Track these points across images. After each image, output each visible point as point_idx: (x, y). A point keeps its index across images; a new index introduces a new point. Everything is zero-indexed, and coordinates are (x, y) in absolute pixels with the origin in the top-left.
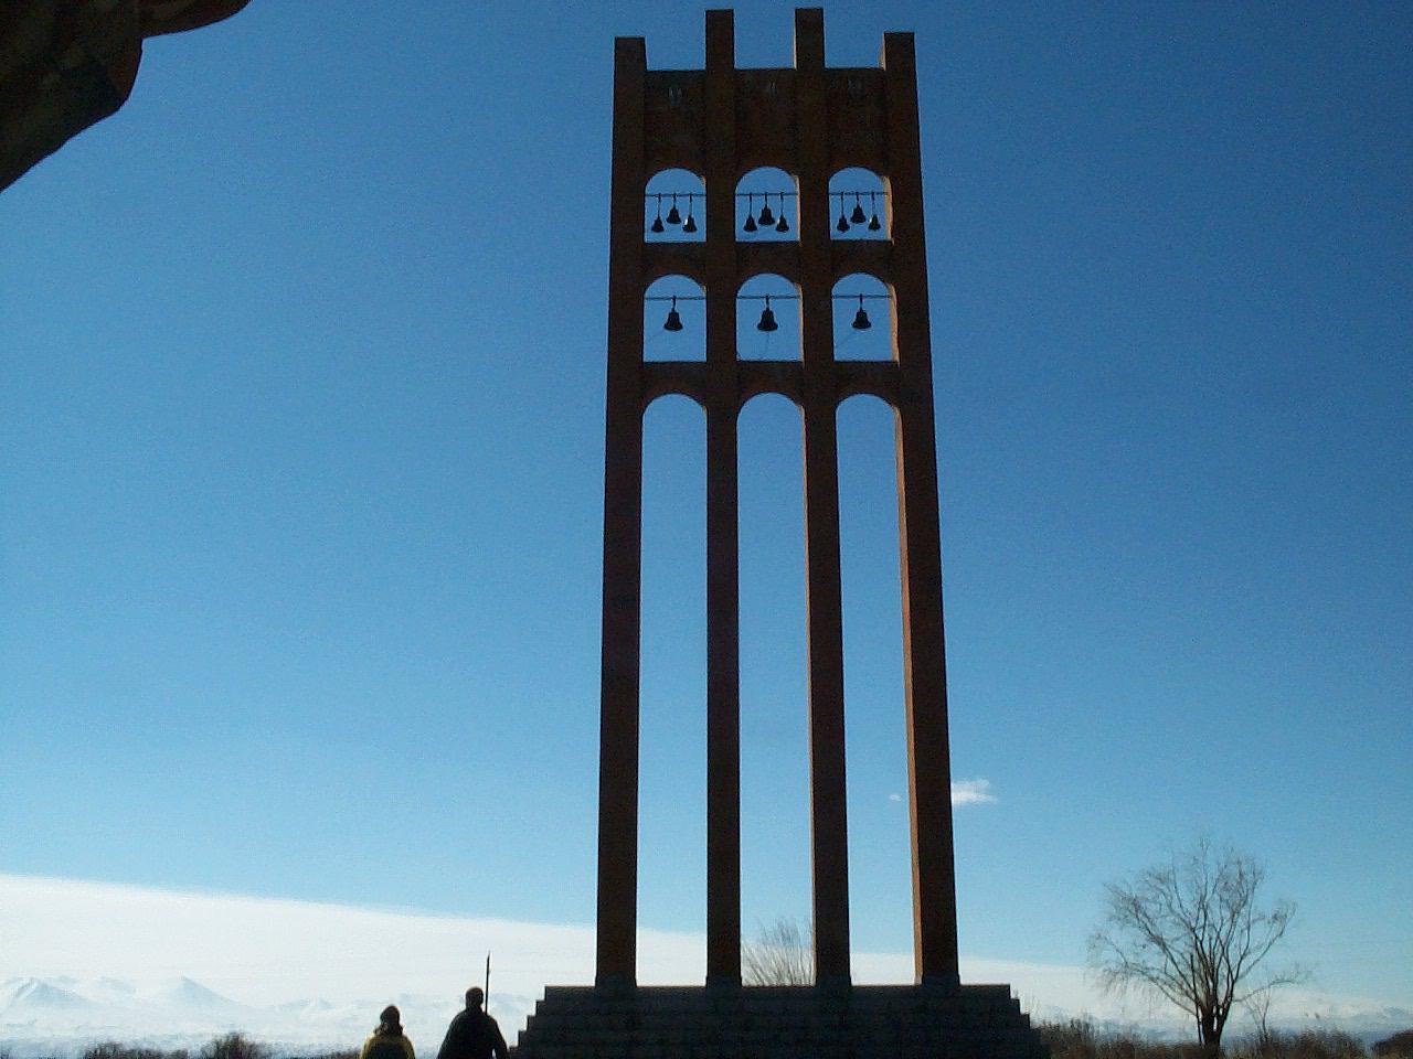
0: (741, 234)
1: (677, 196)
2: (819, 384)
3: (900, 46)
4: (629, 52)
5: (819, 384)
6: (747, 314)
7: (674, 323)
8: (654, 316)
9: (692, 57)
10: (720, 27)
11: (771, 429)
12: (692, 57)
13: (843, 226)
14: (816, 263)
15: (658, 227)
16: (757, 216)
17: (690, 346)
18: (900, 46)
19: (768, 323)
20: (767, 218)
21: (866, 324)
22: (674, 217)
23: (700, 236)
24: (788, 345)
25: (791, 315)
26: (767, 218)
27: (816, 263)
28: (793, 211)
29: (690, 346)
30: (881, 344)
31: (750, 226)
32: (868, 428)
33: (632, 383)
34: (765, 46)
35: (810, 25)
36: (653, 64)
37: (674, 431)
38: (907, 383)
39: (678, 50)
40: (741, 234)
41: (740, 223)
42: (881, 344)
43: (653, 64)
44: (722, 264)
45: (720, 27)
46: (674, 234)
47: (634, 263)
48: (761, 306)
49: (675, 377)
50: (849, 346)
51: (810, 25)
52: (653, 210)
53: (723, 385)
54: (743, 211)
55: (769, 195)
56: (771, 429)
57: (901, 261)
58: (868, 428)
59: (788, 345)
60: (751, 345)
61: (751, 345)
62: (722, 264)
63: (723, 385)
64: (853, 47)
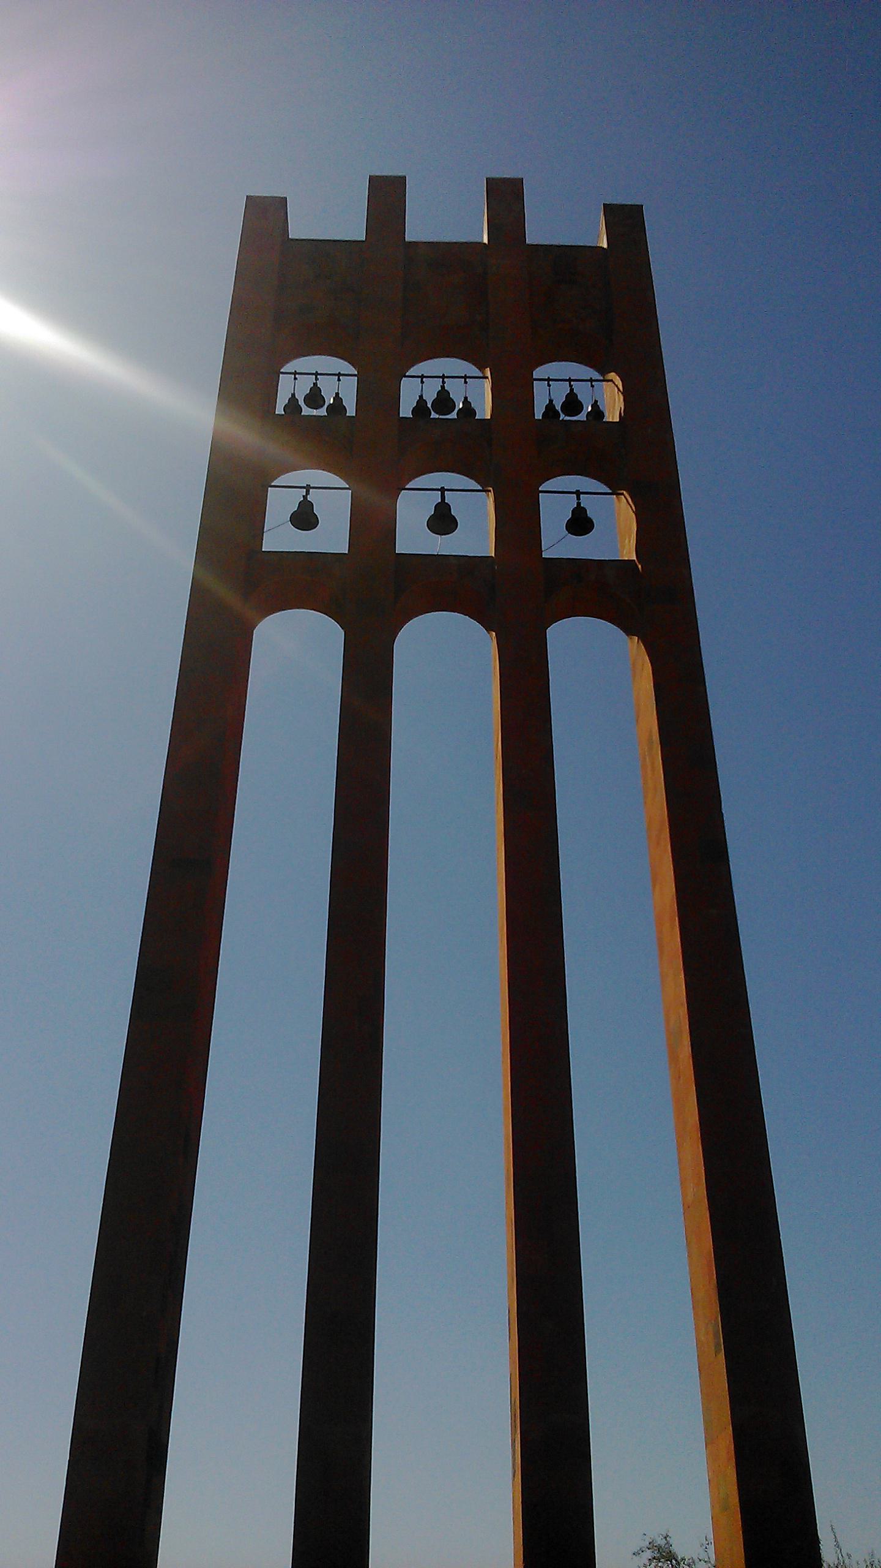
1: (325, 377)
5: (517, 598)
9: (351, 225)
11: (445, 662)
12: (351, 225)
16: (430, 398)
21: (595, 523)
30: (617, 531)
34: (447, 214)
36: (298, 230)
37: (295, 657)
39: (328, 214)
42: (617, 531)
43: (298, 230)
44: (378, 448)
48: (437, 497)
49: (301, 582)
53: (372, 595)
63: (372, 595)
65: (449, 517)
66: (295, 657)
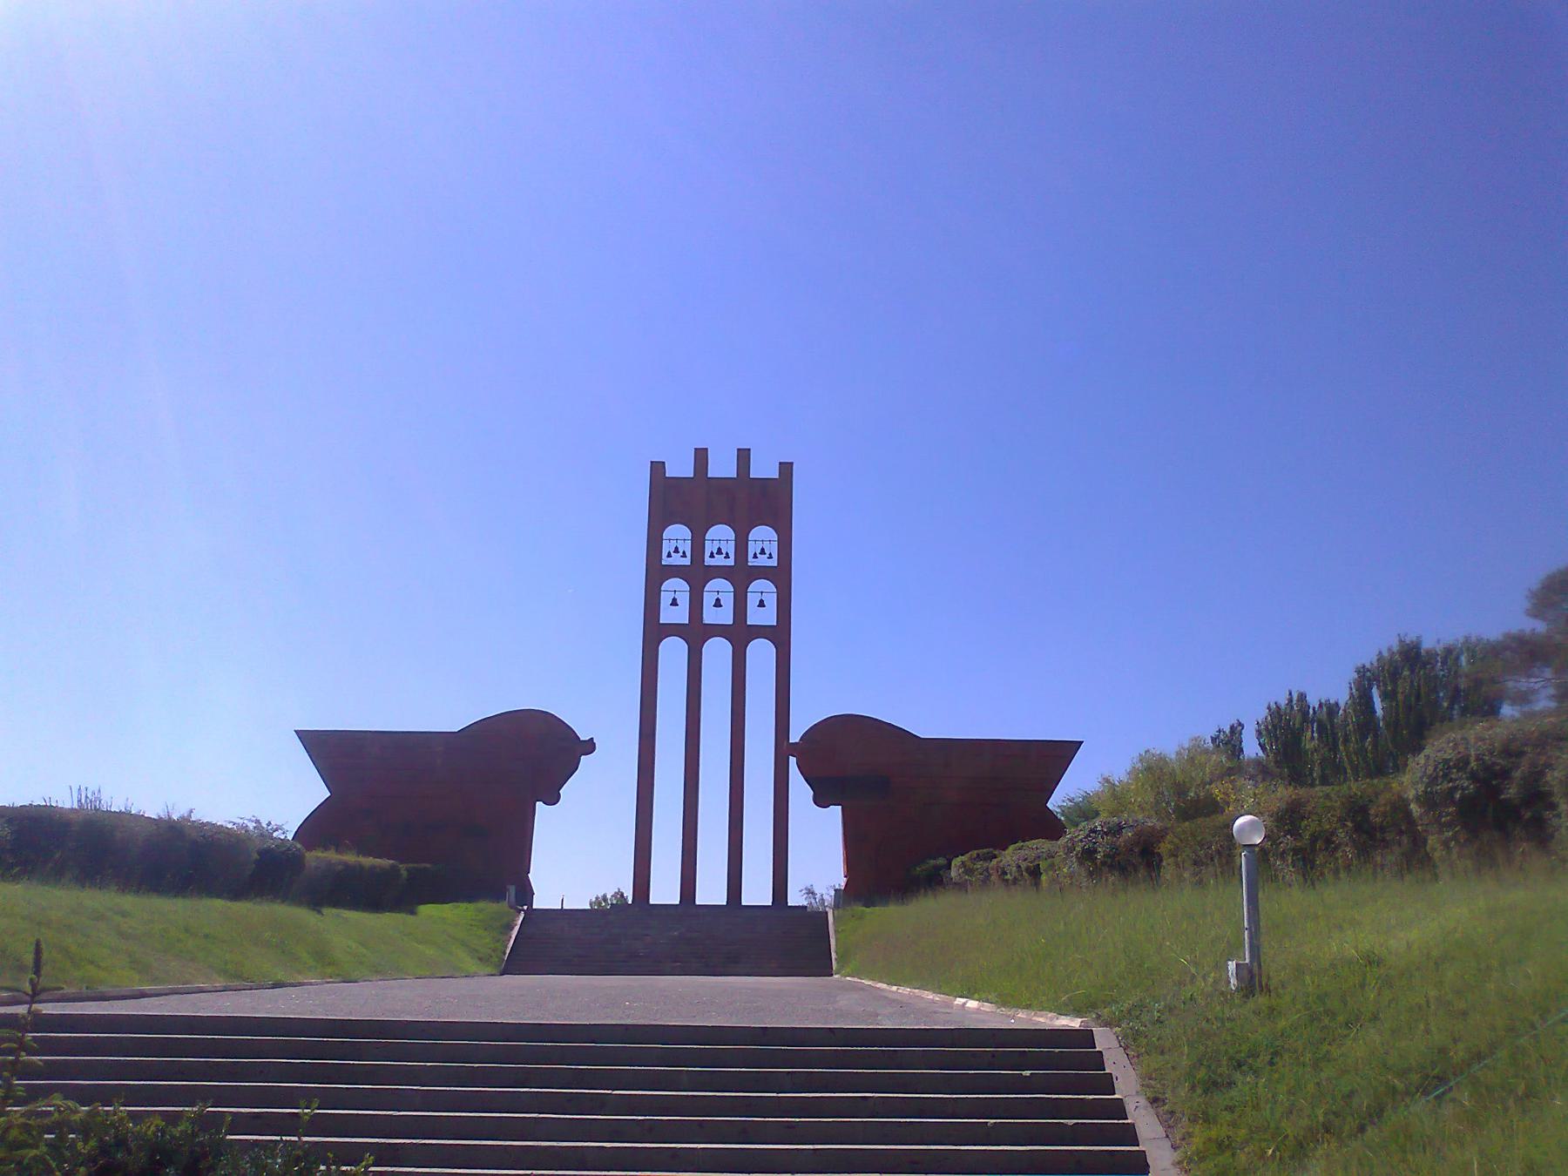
0: (708, 561)
2: (740, 634)
3: (786, 468)
4: (657, 468)
5: (740, 634)
6: (709, 600)
7: (674, 603)
8: (665, 599)
9: (688, 472)
10: (701, 456)
11: (717, 653)
12: (688, 472)
13: (755, 556)
14: (741, 575)
15: (669, 555)
17: (680, 615)
18: (786, 468)
19: (718, 604)
20: (719, 552)
22: (676, 551)
23: (687, 561)
24: (725, 616)
25: (728, 600)
26: (719, 552)
27: (741, 575)
28: (730, 548)
29: (680, 615)
31: (712, 556)
32: (761, 653)
33: (654, 632)
34: (722, 467)
35: (744, 456)
38: (780, 635)
39: (680, 467)
40: (708, 561)
41: (707, 554)
44: (697, 575)
45: (701, 456)
46: (677, 560)
47: (657, 573)
50: (756, 617)
51: (744, 456)
52: (667, 547)
53: (696, 634)
54: (709, 547)
55: (721, 536)
56: (717, 653)
57: (781, 576)
58: (761, 653)
59: (725, 616)
60: (710, 616)
61: (710, 616)
62: (697, 575)
63: (696, 634)
64: (764, 468)
65: (718, 605)
66: (673, 652)
